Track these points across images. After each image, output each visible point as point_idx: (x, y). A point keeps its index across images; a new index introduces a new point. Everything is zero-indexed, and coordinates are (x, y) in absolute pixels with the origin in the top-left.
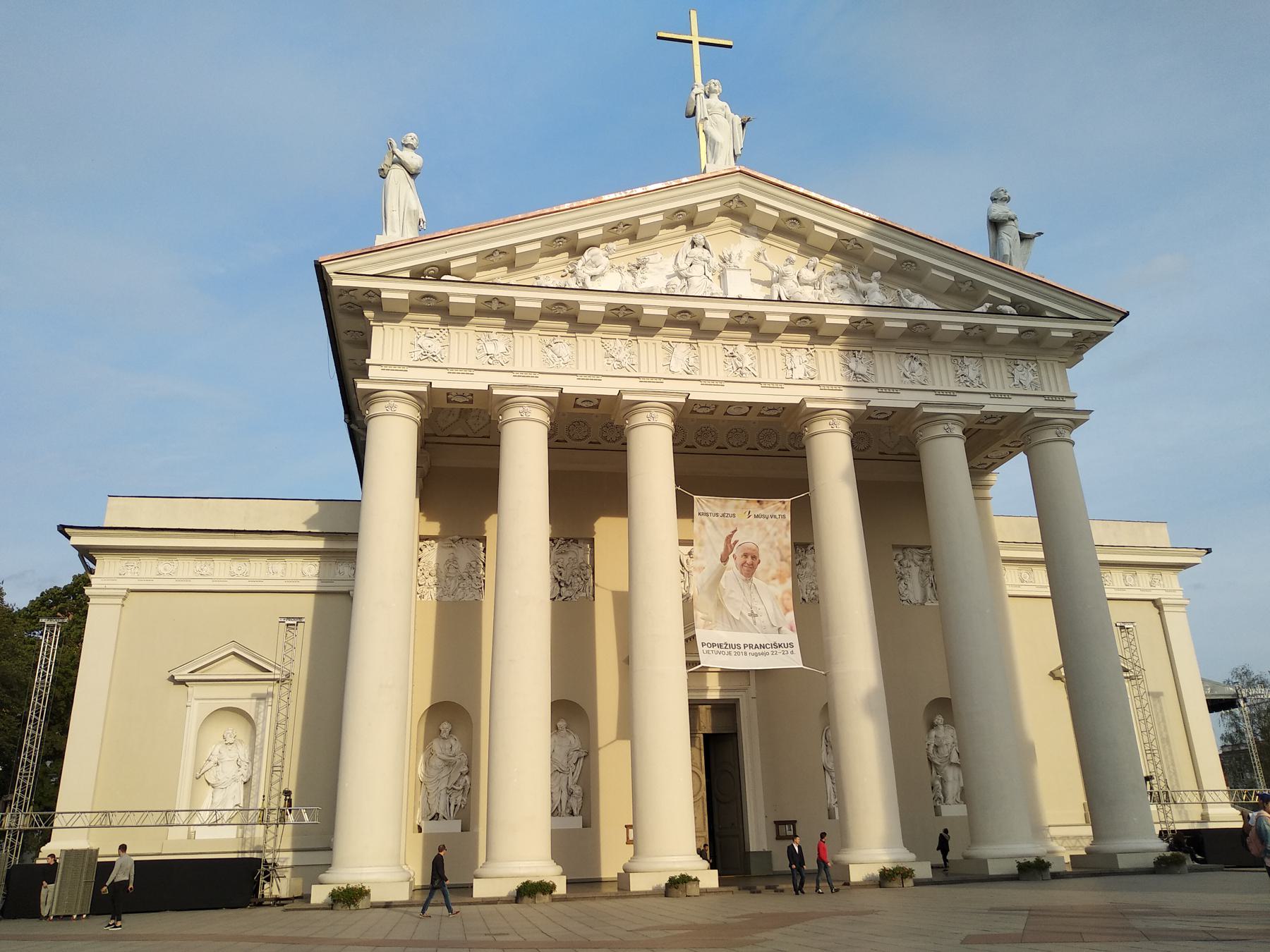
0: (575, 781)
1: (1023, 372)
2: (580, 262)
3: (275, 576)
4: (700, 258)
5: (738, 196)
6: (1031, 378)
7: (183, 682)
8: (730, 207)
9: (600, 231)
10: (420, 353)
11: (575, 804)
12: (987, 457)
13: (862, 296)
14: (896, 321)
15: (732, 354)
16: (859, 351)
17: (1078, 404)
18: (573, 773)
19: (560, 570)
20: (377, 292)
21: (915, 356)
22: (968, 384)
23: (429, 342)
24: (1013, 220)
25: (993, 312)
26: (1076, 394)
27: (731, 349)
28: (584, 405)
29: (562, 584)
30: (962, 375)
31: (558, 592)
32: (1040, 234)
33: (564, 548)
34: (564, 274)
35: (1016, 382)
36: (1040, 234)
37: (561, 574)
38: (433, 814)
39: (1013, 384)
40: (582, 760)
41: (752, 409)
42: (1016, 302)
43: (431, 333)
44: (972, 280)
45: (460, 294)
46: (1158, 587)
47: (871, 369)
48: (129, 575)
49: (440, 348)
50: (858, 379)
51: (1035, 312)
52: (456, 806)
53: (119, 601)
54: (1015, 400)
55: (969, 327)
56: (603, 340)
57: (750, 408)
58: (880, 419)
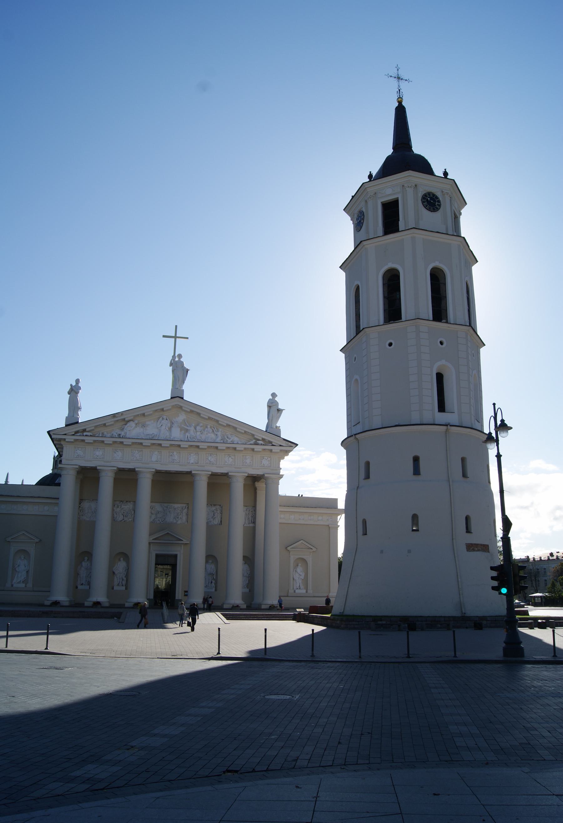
0: (125, 575)
2: (126, 426)
7: (9, 541)
11: (124, 583)
13: (216, 435)
16: (212, 454)
25: (256, 444)
27: (171, 454)
29: (124, 516)
31: (122, 519)
34: (121, 429)
38: (82, 583)
40: (127, 570)
42: (263, 440)
43: (80, 449)
52: (88, 581)
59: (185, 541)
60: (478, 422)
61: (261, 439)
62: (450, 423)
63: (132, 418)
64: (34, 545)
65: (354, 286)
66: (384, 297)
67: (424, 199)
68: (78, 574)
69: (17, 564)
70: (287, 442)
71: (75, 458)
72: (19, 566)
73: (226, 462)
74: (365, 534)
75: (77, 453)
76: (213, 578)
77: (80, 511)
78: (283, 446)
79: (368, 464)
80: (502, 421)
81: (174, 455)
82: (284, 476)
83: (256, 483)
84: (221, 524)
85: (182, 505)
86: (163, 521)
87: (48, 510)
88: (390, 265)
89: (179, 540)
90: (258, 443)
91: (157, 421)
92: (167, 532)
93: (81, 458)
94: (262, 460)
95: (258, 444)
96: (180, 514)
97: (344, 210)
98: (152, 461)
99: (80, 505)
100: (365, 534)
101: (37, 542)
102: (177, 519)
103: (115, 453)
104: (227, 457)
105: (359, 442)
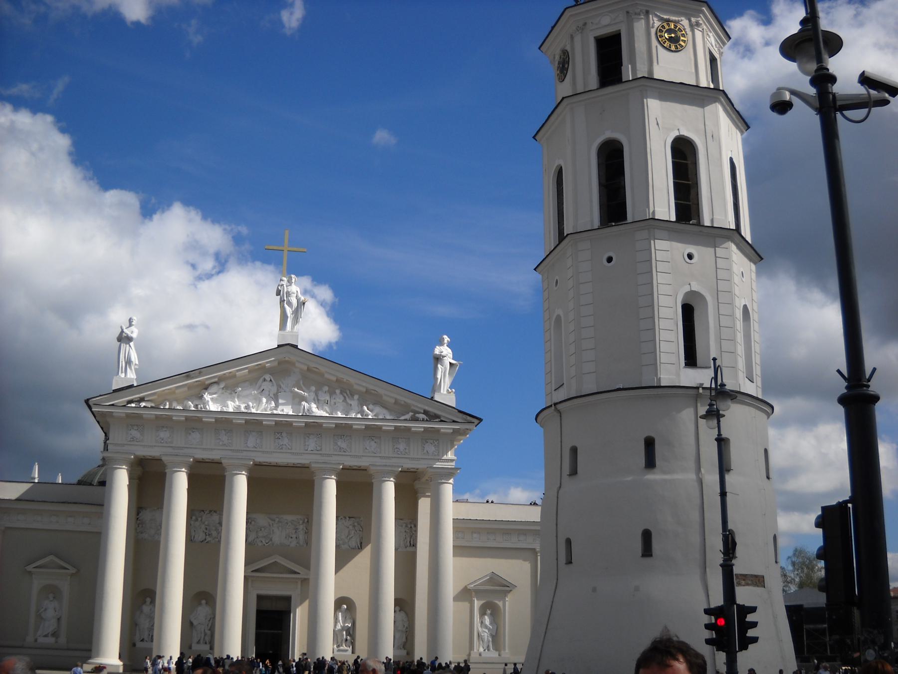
0: (209, 627)
6: (433, 448)
7: (30, 573)
11: (207, 639)
31: (204, 538)
35: (425, 451)
38: (142, 639)
40: (212, 619)
42: (426, 412)
43: (135, 428)
60: (749, 381)
61: (423, 412)
62: (703, 384)
63: (216, 380)
64: (69, 577)
65: (555, 167)
66: (600, 184)
67: (659, 31)
68: (136, 625)
69: (42, 608)
70: (465, 416)
71: (129, 443)
72: (46, 610)
73: (366, 449)
74: (569, 562)
75: (131, 434)
76: (349, 633)
77: (138, 526)
79: (574, 451)
80: (723, 385)
81: (282, 437)
84: (361, 548)
87: (89, 524)
88: (609, 135)
90: (419, 418)
91: (256, 384)
92: (273, 561)
93: (137, 442)
94: (424, 445)
96: (296, 532)
97: (539, 48)
100: (569, 562)
102: (290, 539)
103: (190, 434)
105: (561, 417)
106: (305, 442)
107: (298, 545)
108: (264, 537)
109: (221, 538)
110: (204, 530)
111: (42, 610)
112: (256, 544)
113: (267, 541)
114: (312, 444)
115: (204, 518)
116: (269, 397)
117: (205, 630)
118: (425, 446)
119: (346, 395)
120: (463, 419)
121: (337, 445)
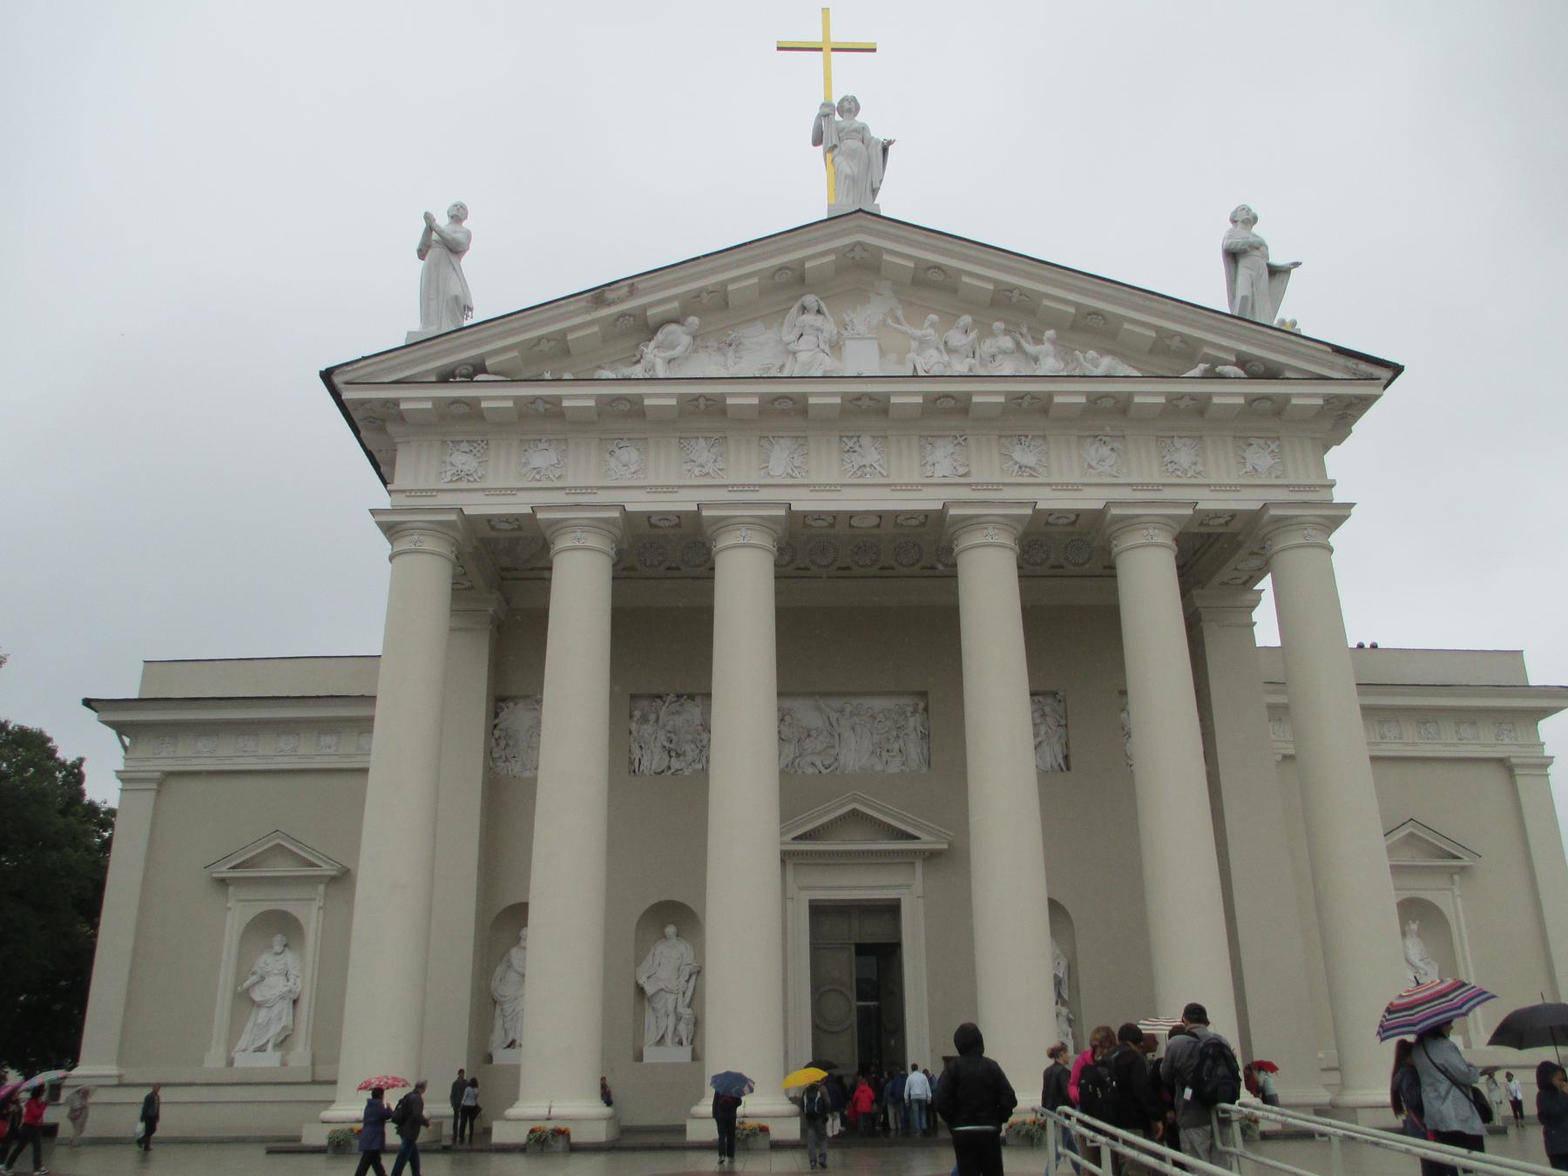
0: (688, 1000)
1: (1258, 455)
2: (652, 344)
3: (327, 751)
4: (811, 326)
5: (860, 243)
7: (223, 882)
8: (853, 258)
9: (676, 304)
10: (452, 472)
11: (684, 1030)
12: (1236, 569)
13: (1033, 363)
14: (1070, 395)
15: (851, 448)
16: (1027, 436)
17: (1339, 496)
18: (684, 993)
19: (669, 735)
20: (395, 402)
21: (1104, 438)
22: (1179, 473)
23: (465, 458)
24: (1257, 248)
25: (1211, 376)
26: (1334, 480)
28: (662, 524)
29: (673, 754)
30: (1171, 462)
31: (665, 765)
32: (1296, 265)
33: (676, 707)
34: (634, 359)
35: (1249, 467)
36: (1296, 265)
37: (671, 741)
39: (1243, 472)
40: (694, 977)
41: (883, 519)
42: (1242, 361)
43: (464, 447)
44: (1180, 334)
45: (494, 396)
46: (1507, 741)
47: (1043, 459)
48: (164, 754)
49: (475, 464)
50: (1025, 474)
51: (1272, 373)
53: (154, 786)
54: (1247, 494)
55: (1173, 398)
56: (682, 441)
57: (880, 517)
58: (1063, 525)
59: (927, 842)
61: (1234, 359)
64: (321, 888)
68: (496, 1002)
69: (254, 973)
70: (1351, 363)
72: (263, 978)
73: (1090, 466)
77: (498, 745)
78: (1332, 379)
82: (1353, 510)
83: (1195, 592)
84: (1068, 769)
85: (902, 701)
86: (830, 766)
89: (901, 839)
93: (468, 481)
94: (1244, 451)
95: (1222, 377)
96: (898, 736)
98: (772, 477)
99: (496, 721)
101: (333, 880)
103: (612, 453)
104: (1091, 445)
106: (925, 456)
107: (903, 768)
108: (819, 753)
109: (708, 762)
110: (666, 744)
111: (253, 979)
112: (799, 772)
113: (825, 763)
114: (943, 460)
115: (662, 714)
116: (818, 350)
117: (676, 1007)
118: (1245, 455)
119: (1019, 336)
120: (1347, 369)
121: (1013, 459)
